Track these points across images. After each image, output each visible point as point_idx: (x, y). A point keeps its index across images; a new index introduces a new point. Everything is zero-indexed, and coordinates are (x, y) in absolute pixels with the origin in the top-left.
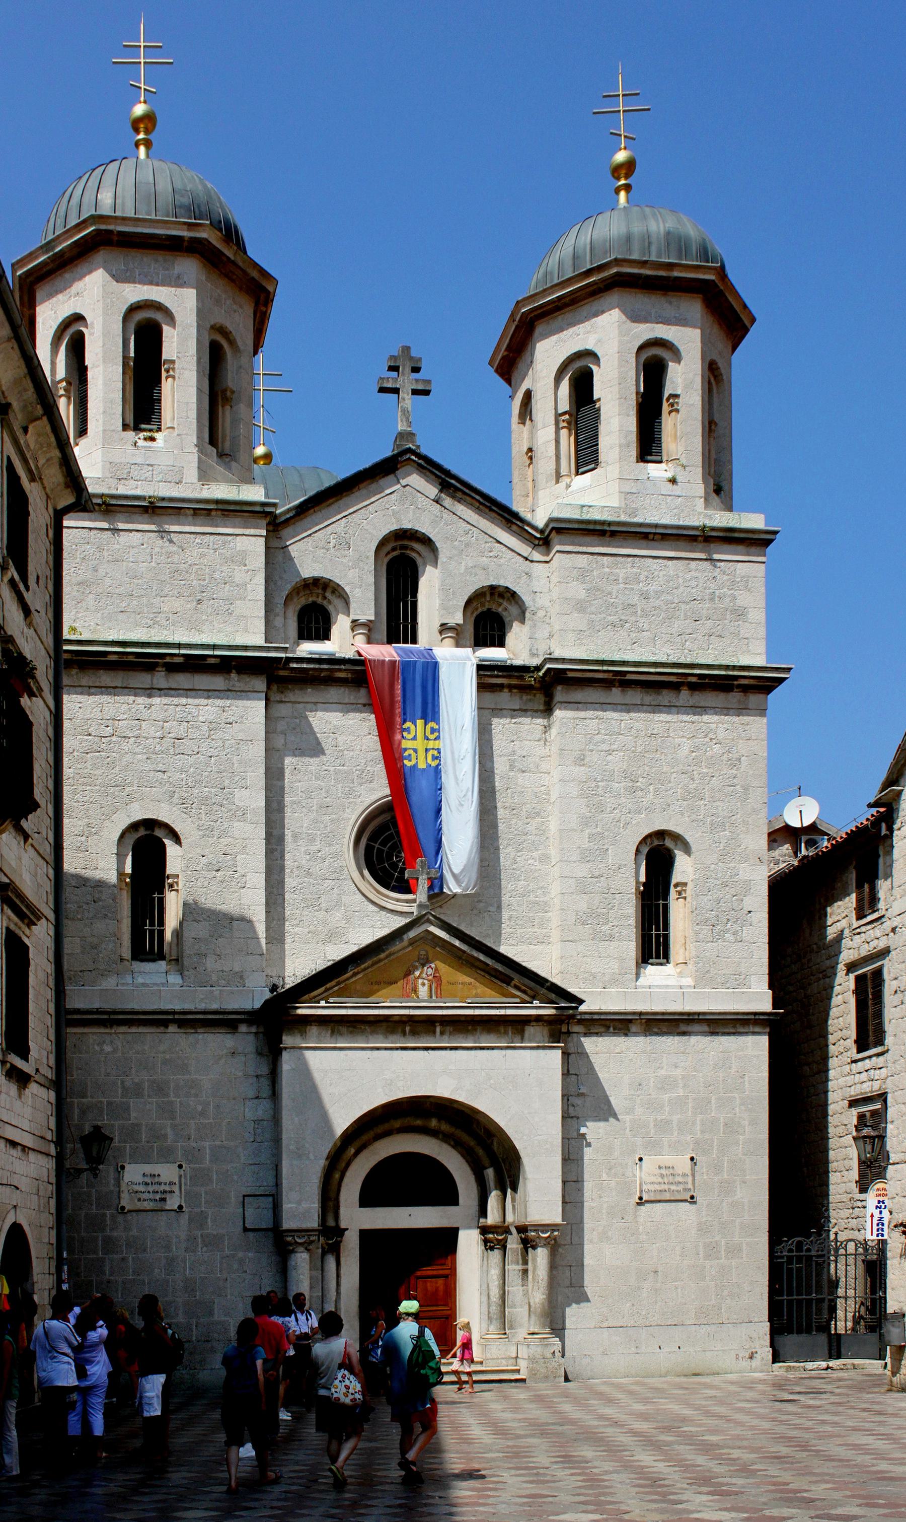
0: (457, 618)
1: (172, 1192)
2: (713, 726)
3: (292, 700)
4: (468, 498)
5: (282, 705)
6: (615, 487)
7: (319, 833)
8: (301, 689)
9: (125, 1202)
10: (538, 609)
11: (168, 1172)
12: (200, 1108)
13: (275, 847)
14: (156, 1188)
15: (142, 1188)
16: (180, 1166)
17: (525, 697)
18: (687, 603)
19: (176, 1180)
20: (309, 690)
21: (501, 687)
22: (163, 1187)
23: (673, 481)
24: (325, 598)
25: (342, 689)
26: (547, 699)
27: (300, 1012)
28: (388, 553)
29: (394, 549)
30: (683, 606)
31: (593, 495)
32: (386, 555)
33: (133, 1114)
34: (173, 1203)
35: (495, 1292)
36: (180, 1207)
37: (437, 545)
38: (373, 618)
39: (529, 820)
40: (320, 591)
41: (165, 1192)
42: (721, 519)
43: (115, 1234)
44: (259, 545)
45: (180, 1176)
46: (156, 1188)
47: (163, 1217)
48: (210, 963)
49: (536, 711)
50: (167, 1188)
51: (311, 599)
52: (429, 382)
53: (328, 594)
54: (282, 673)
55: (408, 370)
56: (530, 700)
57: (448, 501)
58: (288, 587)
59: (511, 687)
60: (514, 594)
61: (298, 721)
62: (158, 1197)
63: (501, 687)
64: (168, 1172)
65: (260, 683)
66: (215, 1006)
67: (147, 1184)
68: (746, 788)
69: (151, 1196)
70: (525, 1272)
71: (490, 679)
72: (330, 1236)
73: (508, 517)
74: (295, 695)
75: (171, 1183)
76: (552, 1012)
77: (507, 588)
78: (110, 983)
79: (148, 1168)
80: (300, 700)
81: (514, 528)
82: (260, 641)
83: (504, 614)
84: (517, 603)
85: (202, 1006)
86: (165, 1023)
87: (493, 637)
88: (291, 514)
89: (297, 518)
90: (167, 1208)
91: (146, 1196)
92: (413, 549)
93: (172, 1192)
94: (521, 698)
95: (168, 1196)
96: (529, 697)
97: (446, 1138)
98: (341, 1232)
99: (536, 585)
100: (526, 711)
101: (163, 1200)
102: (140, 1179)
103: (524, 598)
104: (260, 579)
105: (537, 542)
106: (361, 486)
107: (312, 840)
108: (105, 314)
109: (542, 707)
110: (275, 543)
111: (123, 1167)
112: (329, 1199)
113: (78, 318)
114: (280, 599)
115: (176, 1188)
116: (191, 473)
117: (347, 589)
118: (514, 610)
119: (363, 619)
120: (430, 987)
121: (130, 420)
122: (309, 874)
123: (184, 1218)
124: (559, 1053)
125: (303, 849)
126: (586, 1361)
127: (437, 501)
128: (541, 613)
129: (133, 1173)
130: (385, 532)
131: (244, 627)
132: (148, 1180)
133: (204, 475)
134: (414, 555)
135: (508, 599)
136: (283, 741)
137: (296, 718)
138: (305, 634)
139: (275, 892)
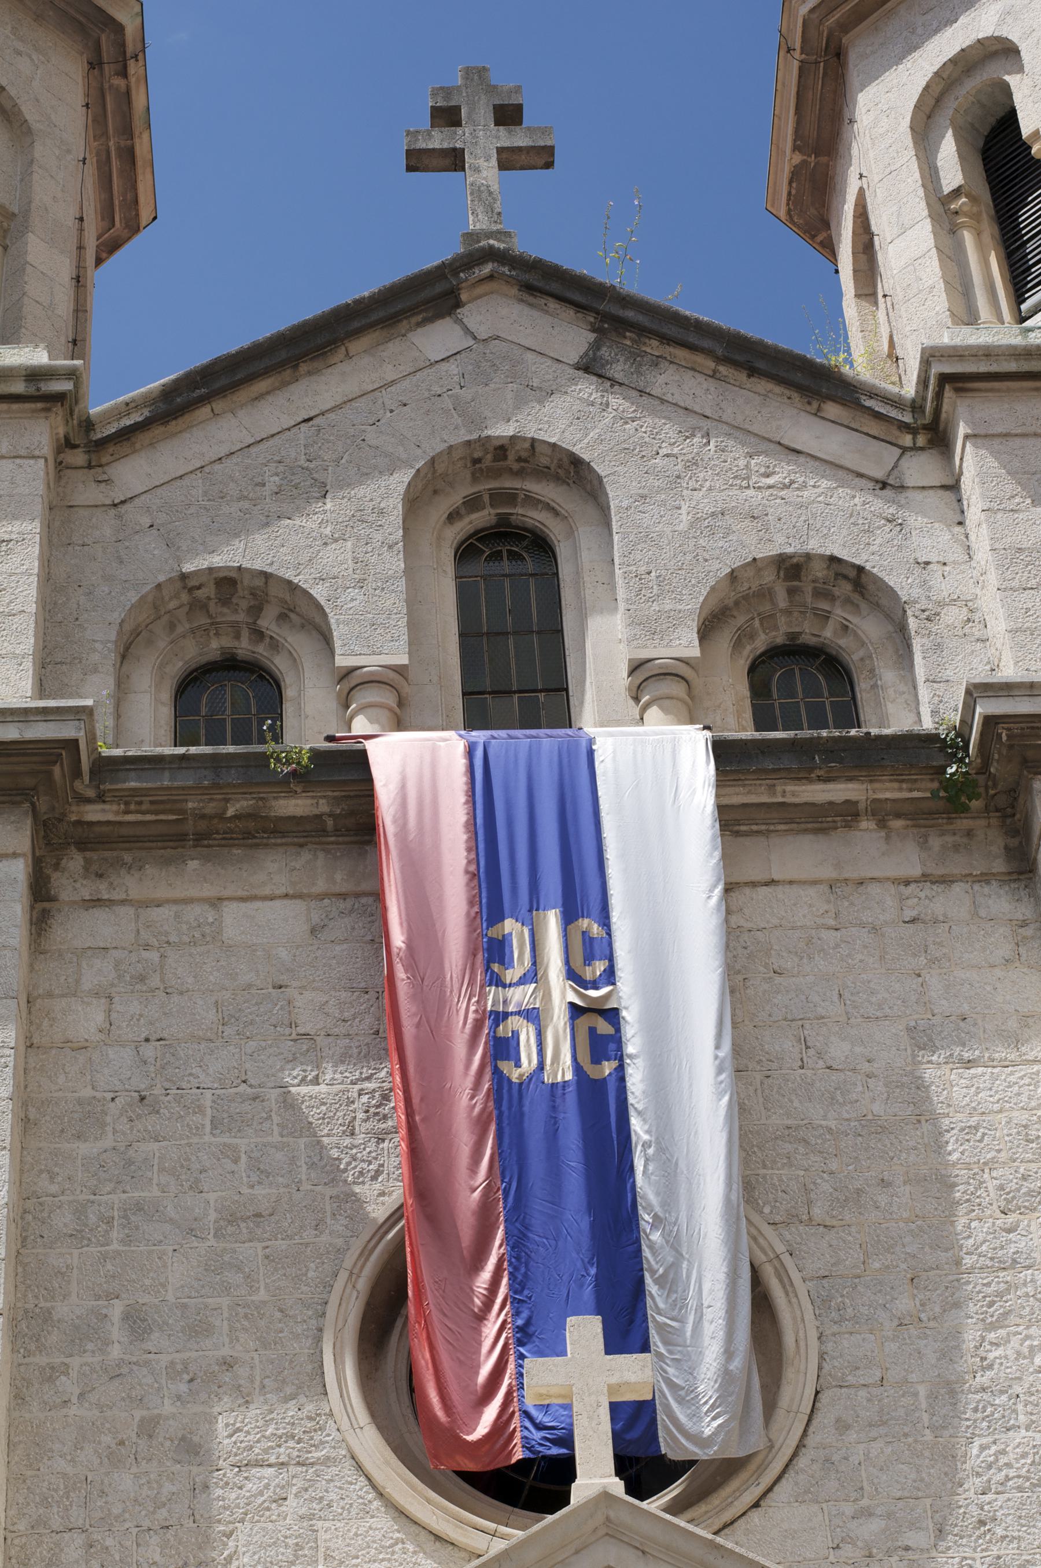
3: (134, 894)
4: (681, 353)
5: (100, 914)
7: (225, 1301)
8: (167, 862)
10: (941, 604)
13: (58, 1359)
17: (936, 842)
20: (193, 864)
21: (847, 815)
24: (259, 635)
25: (306, 856)
26: (1014, 842)
28: (453, 517)
37: (600, 469)
38: (403, 660)
39: (1012, 1218)
40: (241, 617)
49: (985, 878)
51: (215, 644)
52: (545, 131)
53: (267, 622)
54: (94, 813)
55: (484, 114)
56: (956, 848)
59: (882, 814)
61: (154, 956)
63: (847, 815)
74: (150, 881)
77: (833, 559)
80: (162, 892)
81: (832, 410)
84: (877, 606)
88: (137, 417)
89: (158, 431)
92: (531, 501)
94: (923, 844)
96: (949, 839)
100: (945, 881)
103: (891, 581)
105: (907, 440)
106: (355, 346)
107: (199, 1329)
109: (999, 866)
110: (86, 492)
114: (101, 636)
117: (319, 592)
118: (870, 627)
119: (371, 662)
125: (164, 1359)
128: (952, 616)
135: (848, 601)
136: (100, 1018)
137: (147, 947)
139: (56, 1523)
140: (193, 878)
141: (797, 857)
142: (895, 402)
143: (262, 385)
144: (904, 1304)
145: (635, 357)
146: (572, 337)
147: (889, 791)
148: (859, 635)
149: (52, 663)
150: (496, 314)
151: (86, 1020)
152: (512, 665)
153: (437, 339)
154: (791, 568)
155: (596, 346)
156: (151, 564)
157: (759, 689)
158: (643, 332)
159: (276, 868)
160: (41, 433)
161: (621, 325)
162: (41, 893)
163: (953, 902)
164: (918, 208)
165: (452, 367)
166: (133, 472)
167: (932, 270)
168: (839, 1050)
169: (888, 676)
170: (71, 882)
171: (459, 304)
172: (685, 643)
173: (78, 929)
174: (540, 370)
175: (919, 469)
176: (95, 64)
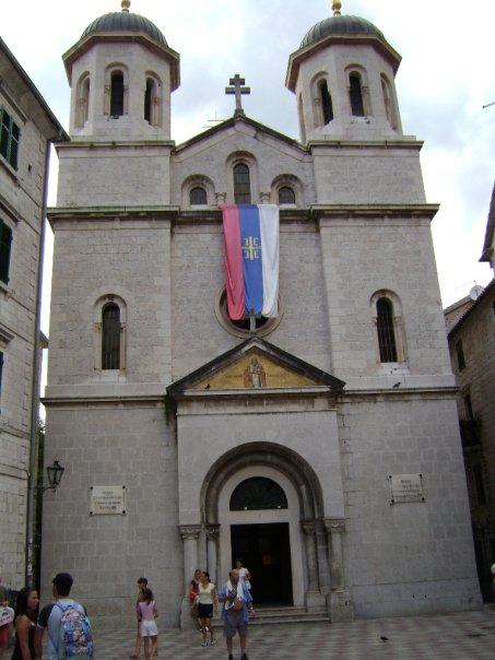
0: (268, 189)
9: (93, 509)
12: (135, 452)
21: (293, 221)
22: (114, 500)
23: (369, 122)
27: (186, 394)
33: (99, 456)
34: (119, 510)
35: (312, 563)
43: (88, 528)
44: (167, 160)
47: (114, 518)
48: (141, 369)
57: (260, 137)
58: (183, 179)
63: (293, 221)
64: (117, 491)
65: (167, 224)
66: (143, 394)
70: (327, 550)
71: (285, 218)
72: (213, 529)
74: (187, 230)
76: (328, 390)
78: (87, 382)
79: (106, 488)
82: (168, 203)
85: (136, 394)
86: (116, 403)
90: (117, 512)
97: (277, 467)
98: (217, 526)
99: (307, 173)
101: (114, 507)
102: (100, 495)
104: (167, 175)
107: (197, 302)
108: (97, 69)
110: (175, 160)
112: (209, 504)
113: (87, 73)
114: (179, 187)
118: (298, 185)
121: (109, 112)
122: (196, 320)
123: (126, 519)
124: (335, 414)
126: (369, 606)
127: (255, 137)
129: (98, 491)
130: (230, 152)
131: (162, 196)
140: (195, 229)
141: (287, 228)
146: (252, 132)
147: (299, 218)
148: (296, 186)
149: (172, 198)
150: (240, 127)
151: (179, 253)
152: (242, 194)
153: (230, 131)
154: (286, 176)
156: (187, 174)
157: (280, 195)
158: (264, 132)
159: (207, 228)
160: (168, 151)
162: (172, 232)
163: (307, 236)
164: (310, 102)
166: (183, 156)
167: (311, 115)
168: (289, 260)
169: (300, 194)
170: (176, 230)
172: (269, 190)
173: (178, 238)
174: (247, 138)
175: (307, 158)
176: (171, 64)
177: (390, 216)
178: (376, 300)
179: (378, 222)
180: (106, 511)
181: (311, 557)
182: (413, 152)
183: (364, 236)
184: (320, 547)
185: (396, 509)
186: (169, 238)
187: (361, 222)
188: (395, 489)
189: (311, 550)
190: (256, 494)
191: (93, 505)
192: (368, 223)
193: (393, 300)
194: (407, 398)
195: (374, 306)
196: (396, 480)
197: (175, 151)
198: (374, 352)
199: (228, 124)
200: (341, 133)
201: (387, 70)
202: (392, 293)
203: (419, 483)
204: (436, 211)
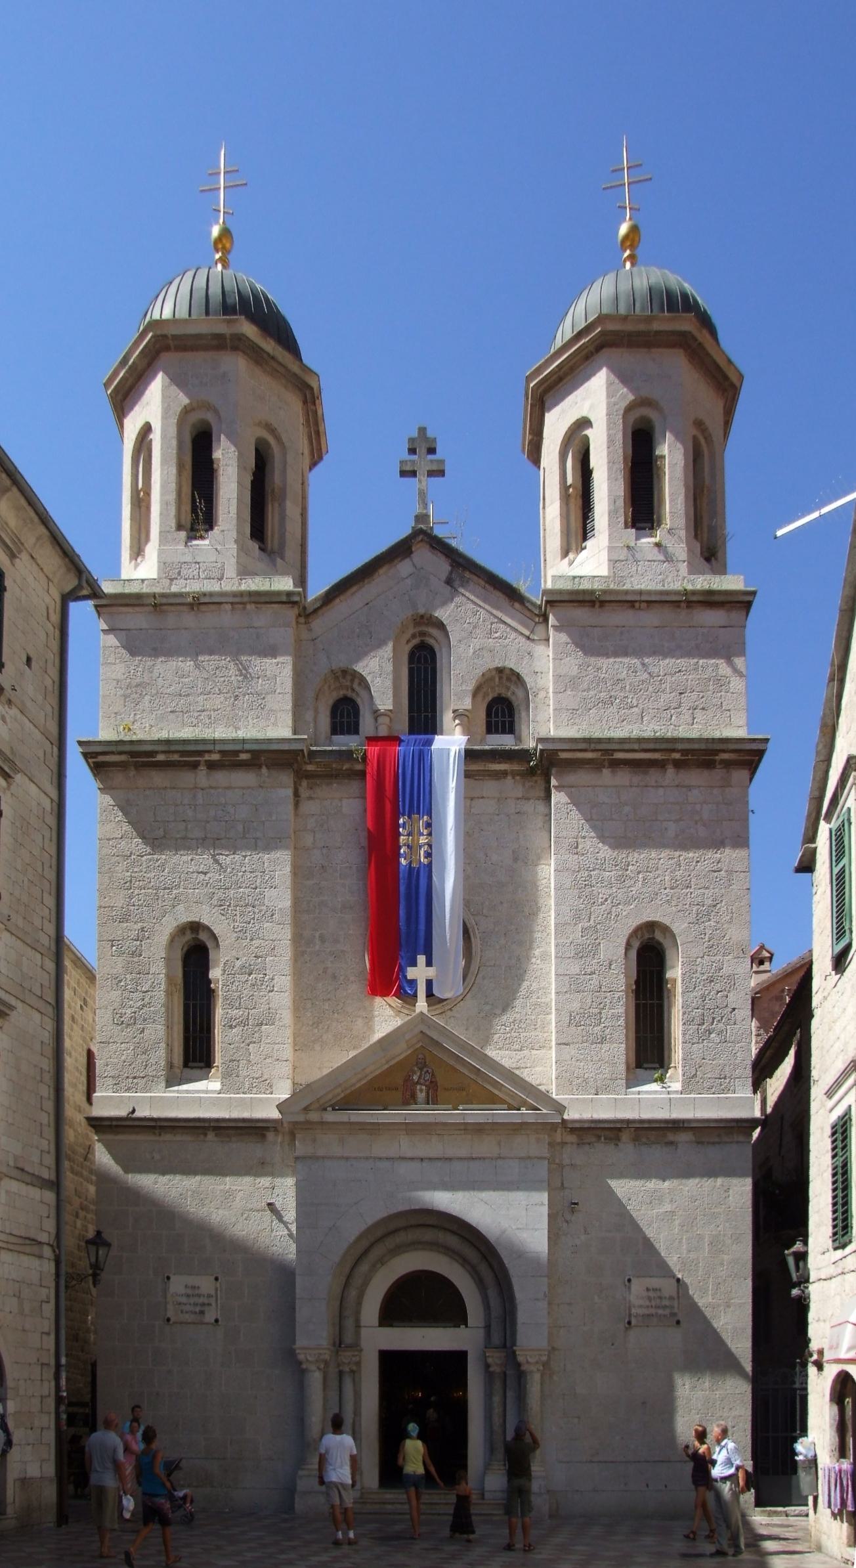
1: (209, 1304)
2: (698, 807)
6: (604, 556)
11: (206, 1284)
14: (196, 1300)
15: (184, 1300)
16: (217, 1279)
17: (528, 784)
18: (672, 675)
19: (213, 1293)
21: (504, 774)
22: (201, 1300)
29: (414, 636)
30: (668, 678)
31: (592, 564)
32: (408, 642)
34: (210, 1317)
36: (217, 1321)
41: (203, 1304)
42: (704, 582)
45: (216, 1290)
46: (196, 1300)
50: (206, 1301)
59: (514, 774)
60: (518, 676)
62: (198, 1309)
63: (504, 774)
64: (206, 1284)
67: (188, 1296)
68: (730, 872)
69: (191, 1308)
73: (511, 594)
75: (209, 1296)
81: (517, 605)
83: (513, 698)
87: (504, 723)
91: (188, 1308)
93: (209, 1304)
94: (524, 785)
95: (206, 1308)
101: (202, 1312)
102: (182, 1290)
111: (168, 1278)
115: (213, 1301)
116: (231, 571)
120: (428, 1093)
127: (449, 582)
129: (178, 1285)
132: (189, 1291)
133: (244, 572)
134: (431, 642)
138: (336, 729)
142: (534, 604)
143: (354, 589)
144: (503, 941)
145: (462, 578)
147: (516, 767)
153: (404, 567)
155: (451, 573)
158: (465, 568)
161: (459, 565)
165: (409, 581)
171: (411, 552)
177: (678, 764)
178: (636, 944)
179: (654, 776)
180: (188, 1318)
181: (497, 1410)
182: (736, 616)
183: (627, 809)
184: (509, 1394)
185: (632, 1333)
186: (291, 807)
187: (623, 777)
188: (632, 1298)
189: (497, 1399)
190: (418, 1299)
191: (170, 1307)
192: (636, 779)
193: (666, 943)
194: (671, 1137)
195: (633, 954)
196: (637, 1286)
197: (307, 614)
198: (618, 1049)
199: (401, 550)
200: (604, 571)
201: (709, 403)
202: (666, 929)
203: (675, 1294)
204: (760, 753)
